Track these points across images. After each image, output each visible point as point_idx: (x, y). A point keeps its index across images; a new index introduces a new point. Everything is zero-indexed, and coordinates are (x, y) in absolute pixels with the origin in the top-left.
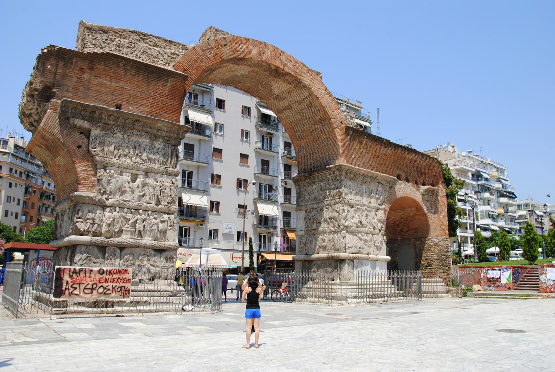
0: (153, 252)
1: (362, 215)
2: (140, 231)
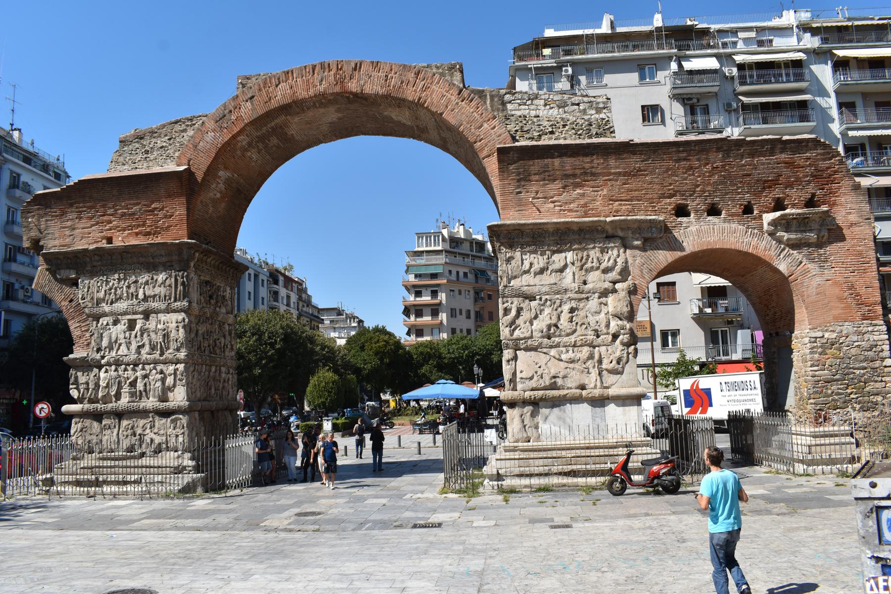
0: (157, 418)
1: (562, 312)
2: (140, 391)
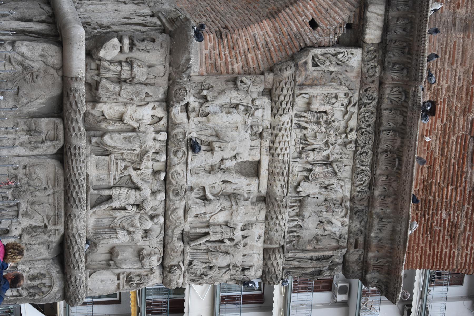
0: (56, 239)
